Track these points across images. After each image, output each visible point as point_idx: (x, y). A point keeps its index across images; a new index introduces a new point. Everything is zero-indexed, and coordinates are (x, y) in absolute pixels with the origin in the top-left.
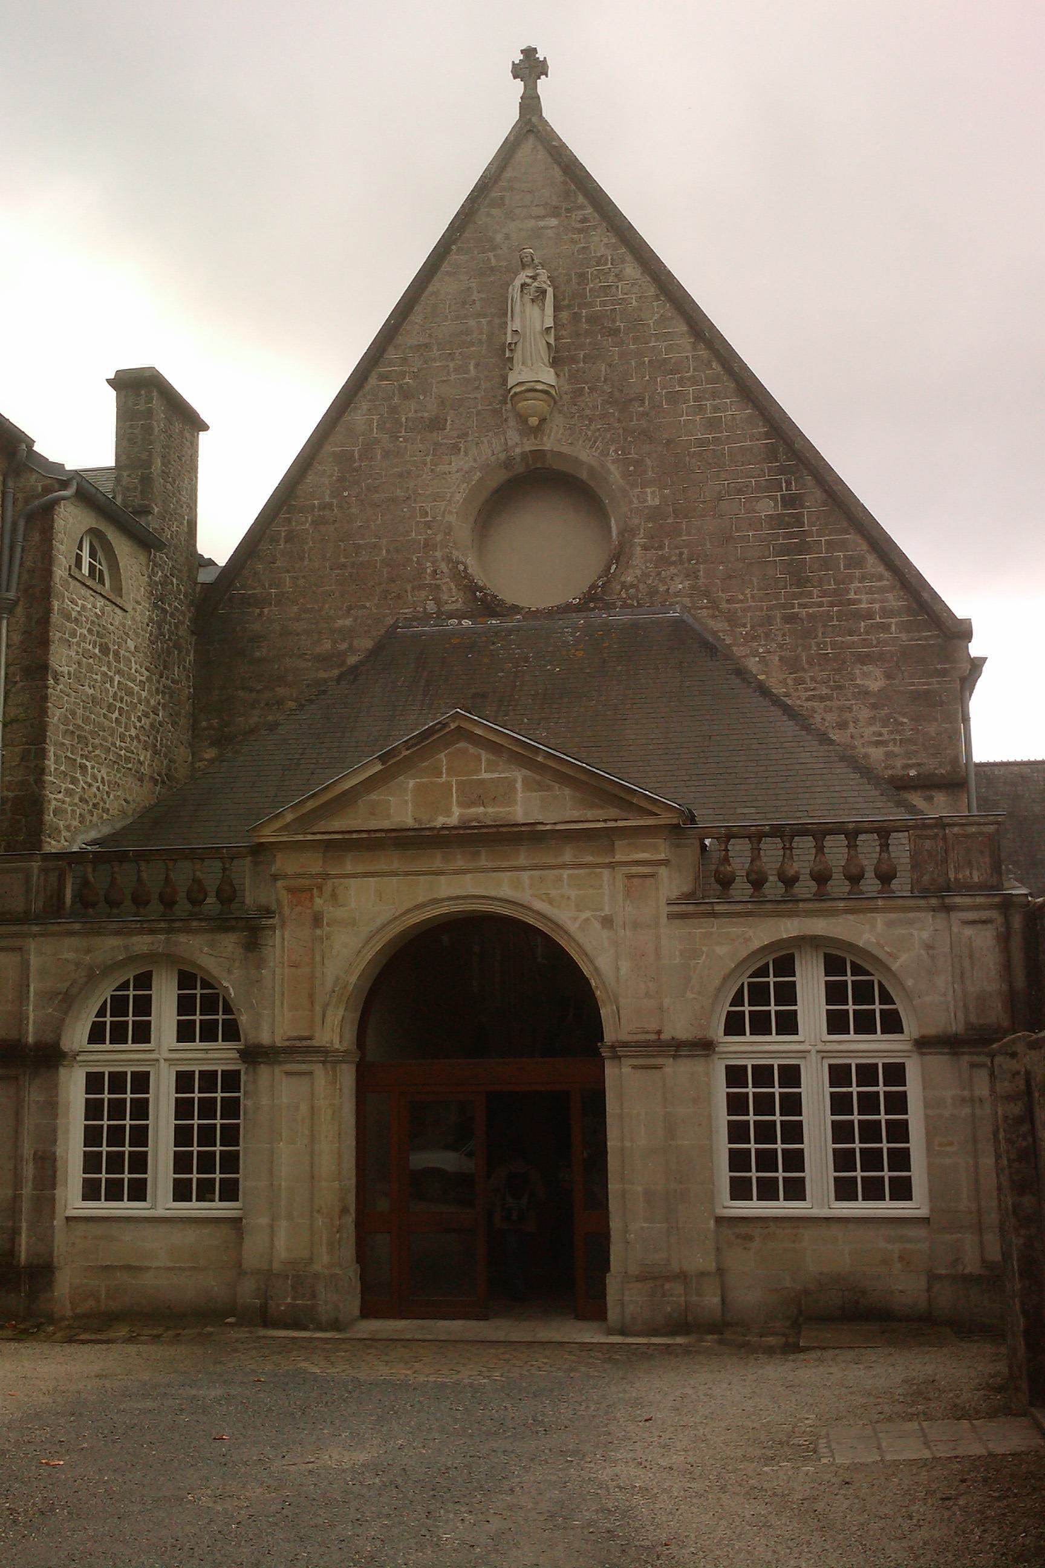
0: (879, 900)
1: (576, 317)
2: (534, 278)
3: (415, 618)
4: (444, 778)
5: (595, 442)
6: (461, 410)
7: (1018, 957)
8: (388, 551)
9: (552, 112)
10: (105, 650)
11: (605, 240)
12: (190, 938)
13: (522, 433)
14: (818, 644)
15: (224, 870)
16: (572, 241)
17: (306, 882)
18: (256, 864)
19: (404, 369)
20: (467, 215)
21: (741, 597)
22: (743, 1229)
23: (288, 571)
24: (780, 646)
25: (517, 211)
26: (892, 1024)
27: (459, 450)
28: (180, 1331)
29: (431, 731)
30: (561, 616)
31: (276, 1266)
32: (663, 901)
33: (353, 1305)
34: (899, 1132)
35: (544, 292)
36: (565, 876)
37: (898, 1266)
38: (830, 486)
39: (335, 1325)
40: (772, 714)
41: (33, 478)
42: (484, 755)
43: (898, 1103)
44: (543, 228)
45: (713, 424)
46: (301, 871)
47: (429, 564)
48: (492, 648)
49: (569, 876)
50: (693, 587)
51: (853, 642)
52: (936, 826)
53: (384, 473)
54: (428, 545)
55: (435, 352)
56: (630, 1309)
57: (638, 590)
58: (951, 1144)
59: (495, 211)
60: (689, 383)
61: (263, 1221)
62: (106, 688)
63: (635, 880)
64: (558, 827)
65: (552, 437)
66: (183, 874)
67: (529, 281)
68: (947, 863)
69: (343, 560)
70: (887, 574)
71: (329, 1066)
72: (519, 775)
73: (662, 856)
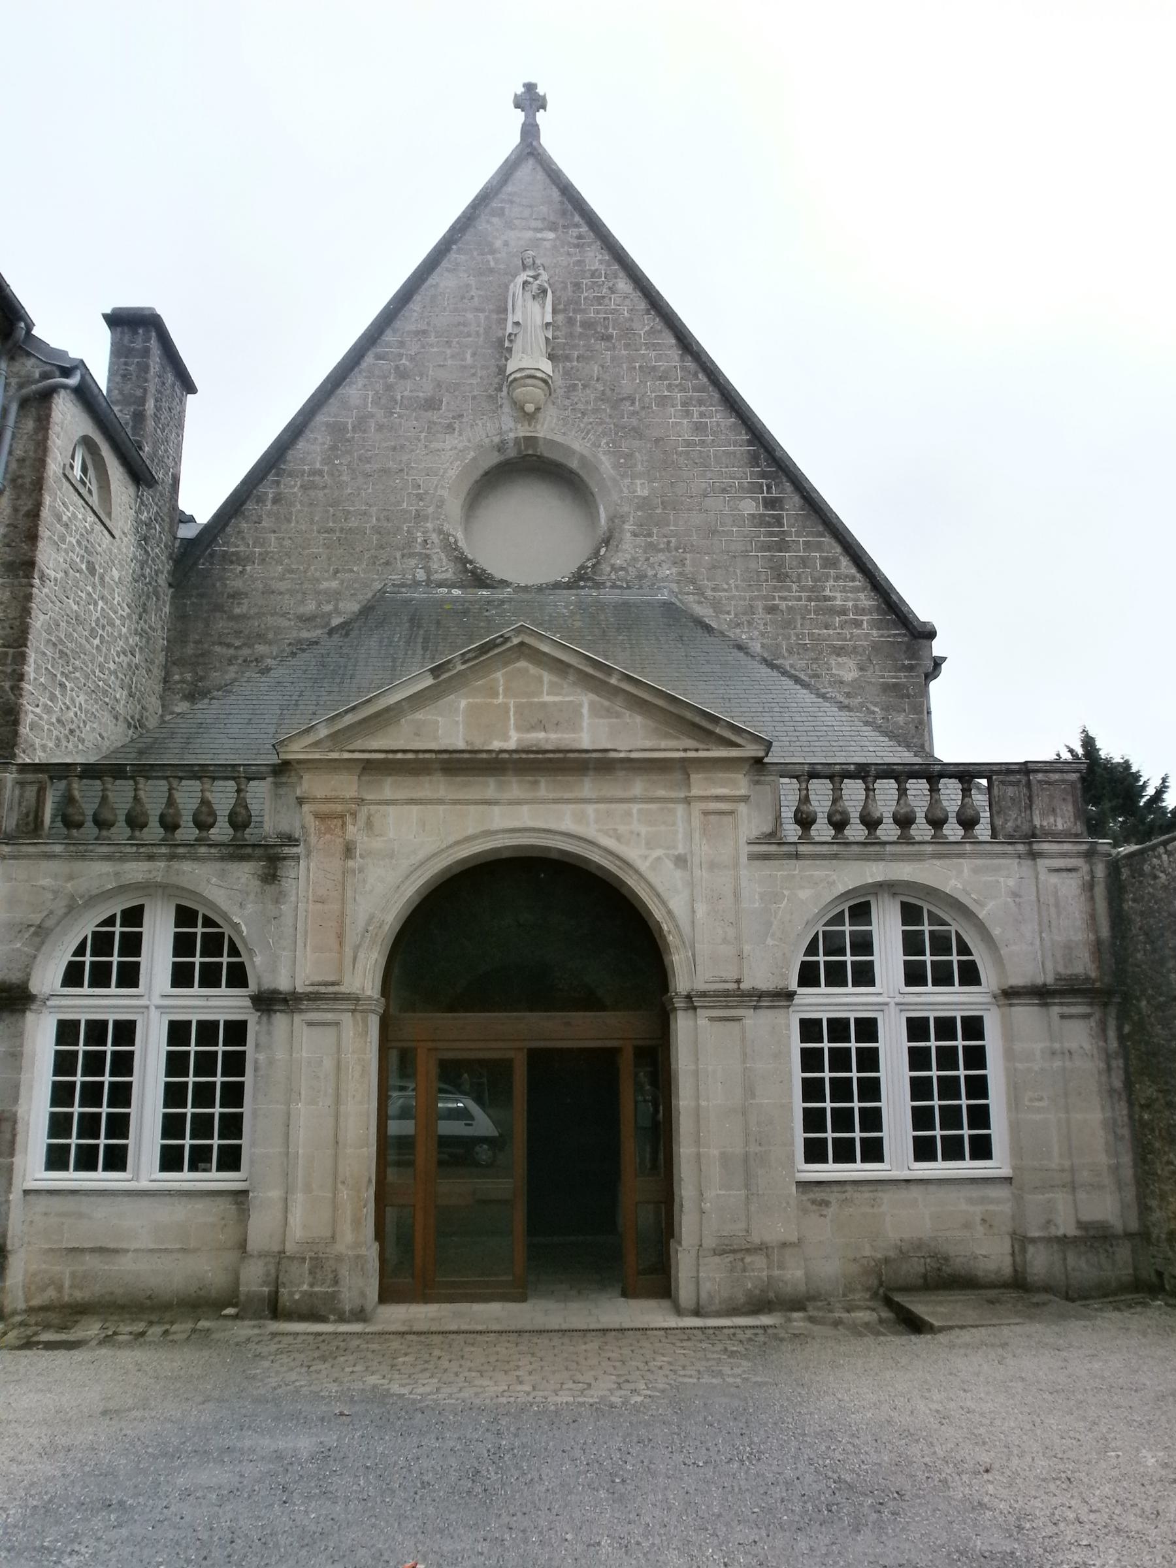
0: (967, 845)
1: (570, 322)
2: (535, 277)
3: (403, 585)
4: (501, 699)
5: (588, 433)
6: (457, 393)
7: (1102, 906)
8: (378, 519)
9: (550, 142)
10: (92, 569)
11: (600, 257)
12: (195, 866)
13: (516, 420)
14: (797, 635)
15: (238, 791)
16: (569, 254)
17: (339, 808)
18: (277, 785)
19: (402, 351)
20: (469, 219)
21: (726, 586)
22: (818, 1194)
23: (274, 532)
24: (762, 634)
25: (516, 222)
26: (970, 975)
27: (454, 429)
28: (167, 1327)
29: (491, 645)
30: (551, 592)
31: (290, 1248)
32: (743, 840)
33: (373, 1292)
34: (978, 1087)
35: (545, 291)
36: (635, 811)
37: (980, 1229)
38: (807, 492)
39: (360, 1315)
40: (784, 683)
41: (30, 362)
42: (547, 677)
43: (976, 1058)
44: (541, 239)
45: (699, 428)
46: (333, 794)
47: (419, 534)
48: (486, 614)
49: (640, 811)
50: (680, 574)
51: (829, 635)
52: (1019, 772)
53: (377, 445)
54: (419, 517)
55: (432, 339)
56: (706, 1287)
57: (627, 572)
58: (1041, 1099)
59: (495, 220)
60: (676, 390)
61: (275, 1194)
62: (89, 609)
63: (712, 818)
64: (634, 755)
65: (545, 426)
66: (188, 795)
67: (531, 280)
68: (1031, 809)
69: (331, 524)
70: (858, 576)
71: (358, 1016)
72: (585, 700)
73: (743, 792)
